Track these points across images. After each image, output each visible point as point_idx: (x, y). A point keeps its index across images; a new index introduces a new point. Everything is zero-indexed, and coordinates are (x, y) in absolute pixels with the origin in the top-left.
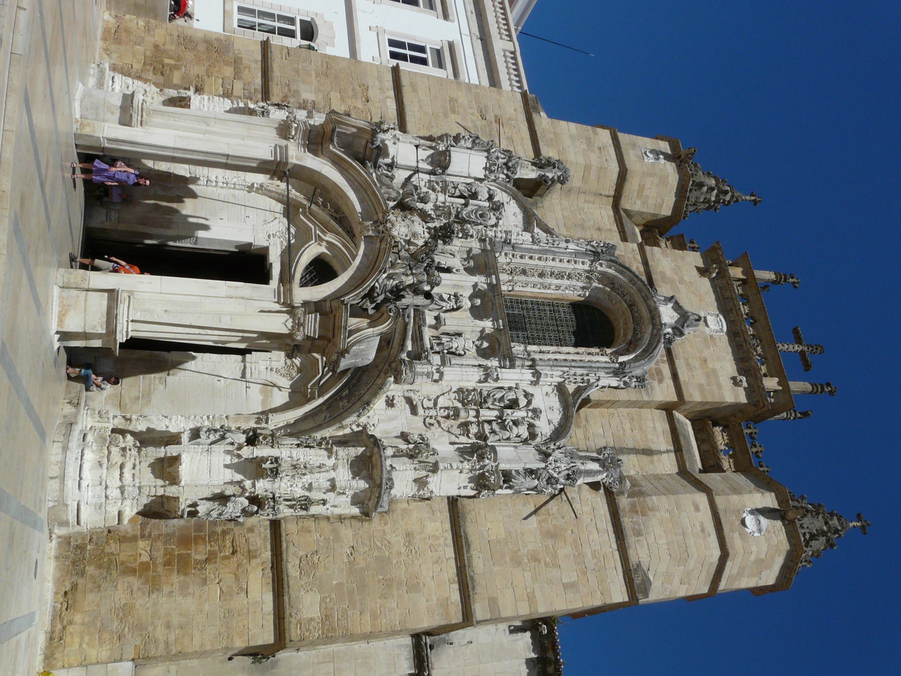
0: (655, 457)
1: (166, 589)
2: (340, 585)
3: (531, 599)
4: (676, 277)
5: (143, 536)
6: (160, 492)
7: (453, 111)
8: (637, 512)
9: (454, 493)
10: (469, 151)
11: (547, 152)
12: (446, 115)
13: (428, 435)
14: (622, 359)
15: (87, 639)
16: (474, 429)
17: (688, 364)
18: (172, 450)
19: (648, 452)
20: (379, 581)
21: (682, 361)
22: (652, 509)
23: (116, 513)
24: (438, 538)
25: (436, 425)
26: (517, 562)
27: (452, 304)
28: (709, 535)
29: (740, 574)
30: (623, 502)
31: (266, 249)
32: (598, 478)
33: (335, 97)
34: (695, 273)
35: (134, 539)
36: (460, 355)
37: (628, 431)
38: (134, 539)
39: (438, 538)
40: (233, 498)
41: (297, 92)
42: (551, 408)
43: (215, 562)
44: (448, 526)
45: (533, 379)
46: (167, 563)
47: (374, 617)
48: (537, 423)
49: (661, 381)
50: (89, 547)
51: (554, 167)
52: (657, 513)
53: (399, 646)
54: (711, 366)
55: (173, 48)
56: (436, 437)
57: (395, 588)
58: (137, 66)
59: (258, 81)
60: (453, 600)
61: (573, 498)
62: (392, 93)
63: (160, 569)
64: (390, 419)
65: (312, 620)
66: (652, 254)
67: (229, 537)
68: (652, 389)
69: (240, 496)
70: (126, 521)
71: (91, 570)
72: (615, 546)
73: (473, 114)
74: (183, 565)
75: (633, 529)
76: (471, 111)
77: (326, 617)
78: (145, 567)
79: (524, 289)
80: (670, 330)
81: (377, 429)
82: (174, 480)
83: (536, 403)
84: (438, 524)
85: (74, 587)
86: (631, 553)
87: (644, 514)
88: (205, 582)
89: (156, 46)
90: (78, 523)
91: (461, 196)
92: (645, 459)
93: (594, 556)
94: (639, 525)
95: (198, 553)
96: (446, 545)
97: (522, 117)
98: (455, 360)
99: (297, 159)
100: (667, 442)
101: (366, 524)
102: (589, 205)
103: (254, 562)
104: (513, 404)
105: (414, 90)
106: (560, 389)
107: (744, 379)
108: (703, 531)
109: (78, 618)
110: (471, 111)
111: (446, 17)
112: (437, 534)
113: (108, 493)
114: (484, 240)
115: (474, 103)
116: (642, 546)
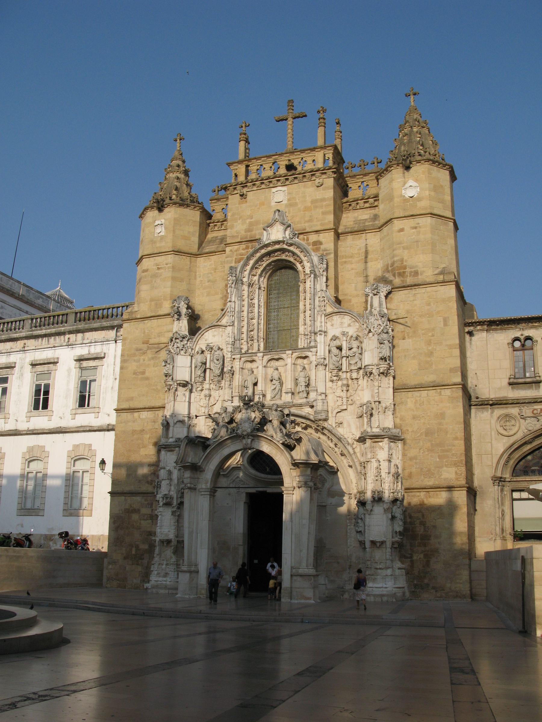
0: (369, 248)
2: (439, 456)
3: (450, 347)
4: (248, 221)
5: (411, 557)
6: (389, 550)
7: (143, 373)
8: (404, 272)
9: (391, 390)
10: (175, 368)
11: (166, 308)
12: (147, 379)
13: (358, 403)
14: (308, 271)
15: (458, 581)
16: (355, 375)
17: (309, 221)
18: (368, 545)
19: (367, 253)
20: (438, 435)
21: (306, 224)
22: (402, 260)
23: (399, 570)
24: (416, 400)
25: (352, 397)
26: (431, 354)
27: (277, 383)
28: (418, 224)
29: (442, 201)
30: (397, 281)
31: (247, 493)
32: (384, 298)
34: (244, 206)
35: (412, 562)
36: (309, 380)
37: (353, 266)
38: (412, 562)
39: (416, 400)
40: (393, 514)
42: (342, 323)
43: (425, 522)
44: (410, 394)
45: (323, 335)
46: (425, 545)
47: (456, 438)
48: (350, 334)
49: (321, 243)
50: (415, 582)
51: (179, 307)
52: (405, 258)
53: (476, 416)
54: (309, 204)
55: (124, 549)
56: (359, 398)
57: (442, 427)
58: (140, 568)
59: (138, 499)
60: (450, 394)
61: (395, 314)
62: (136, 415)
64: (349, 425)
65: (456, 473)
66: (233, 237)
67: (413, 515)
68: (326, 250)
69: (392, 510)
70: (403, 566)
71: (426, 581)
72: (423, 290)
73: (144, 360)
74: (426, 538)
75: (414, 276)
76: (142, 361)
77: (455, 464)
78: (426, 556)
79: (262, 330)
80: (287, 232)
81: (355, 434)
82: (383, 543)
83: (338, 334)
84: (409, 400)
85: (434, 588)
86: (428, 280)
87: (405, 268)
88: (434, 527)
89: (125, 558)
90: (403, 588)
91: (205, 371)
92: (369, 257)
93: (429, 304)
94: (411, 272)
95: (420, 530)
96: (420, 396)
97: (141, 325)
98: (313, 383)
99: (206, 483)
100: (359, 239)
101: (408, 441)
102: (198, 276)
104: (340, 348)
105: (132, 399)
106: (329, 315)
107: (317, 181)
108: (416, 228)
109: (448, 585)
110: (142, 360)
111: (55, 363)
112: (414, 401)
113: (389, 574)
114: (234, 359)
115: (136, 358)
116: (424, 272)
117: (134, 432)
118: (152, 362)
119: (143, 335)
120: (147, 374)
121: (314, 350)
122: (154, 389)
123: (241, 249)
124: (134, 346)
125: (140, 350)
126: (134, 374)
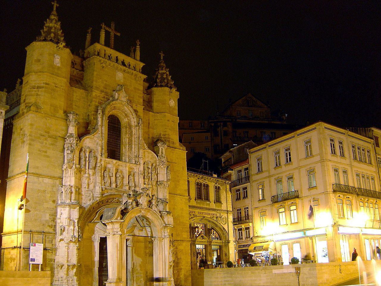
1: (182, 267)
7: (46, 152)
12: (48, 157)
19: (149, 123)
22: (169, 134)
31: (100, 237)
33: (46, 205)
41: (46, 221)
62: (40, 179)
63: (178, 268)
76: (44, 144)
88: (181, 258)
103: (178, 248)
105: (37, 168)
108: (173, 122)
110: (44, 144)
117: (39, 191)
118: (51, 146)
119: (45, 126)
120: (48, 154)
121: (138, 166)
122: (53, 165)
123: (101, 96)
124: (39, 132)
125: (44, 136)
126: (39, 151)
